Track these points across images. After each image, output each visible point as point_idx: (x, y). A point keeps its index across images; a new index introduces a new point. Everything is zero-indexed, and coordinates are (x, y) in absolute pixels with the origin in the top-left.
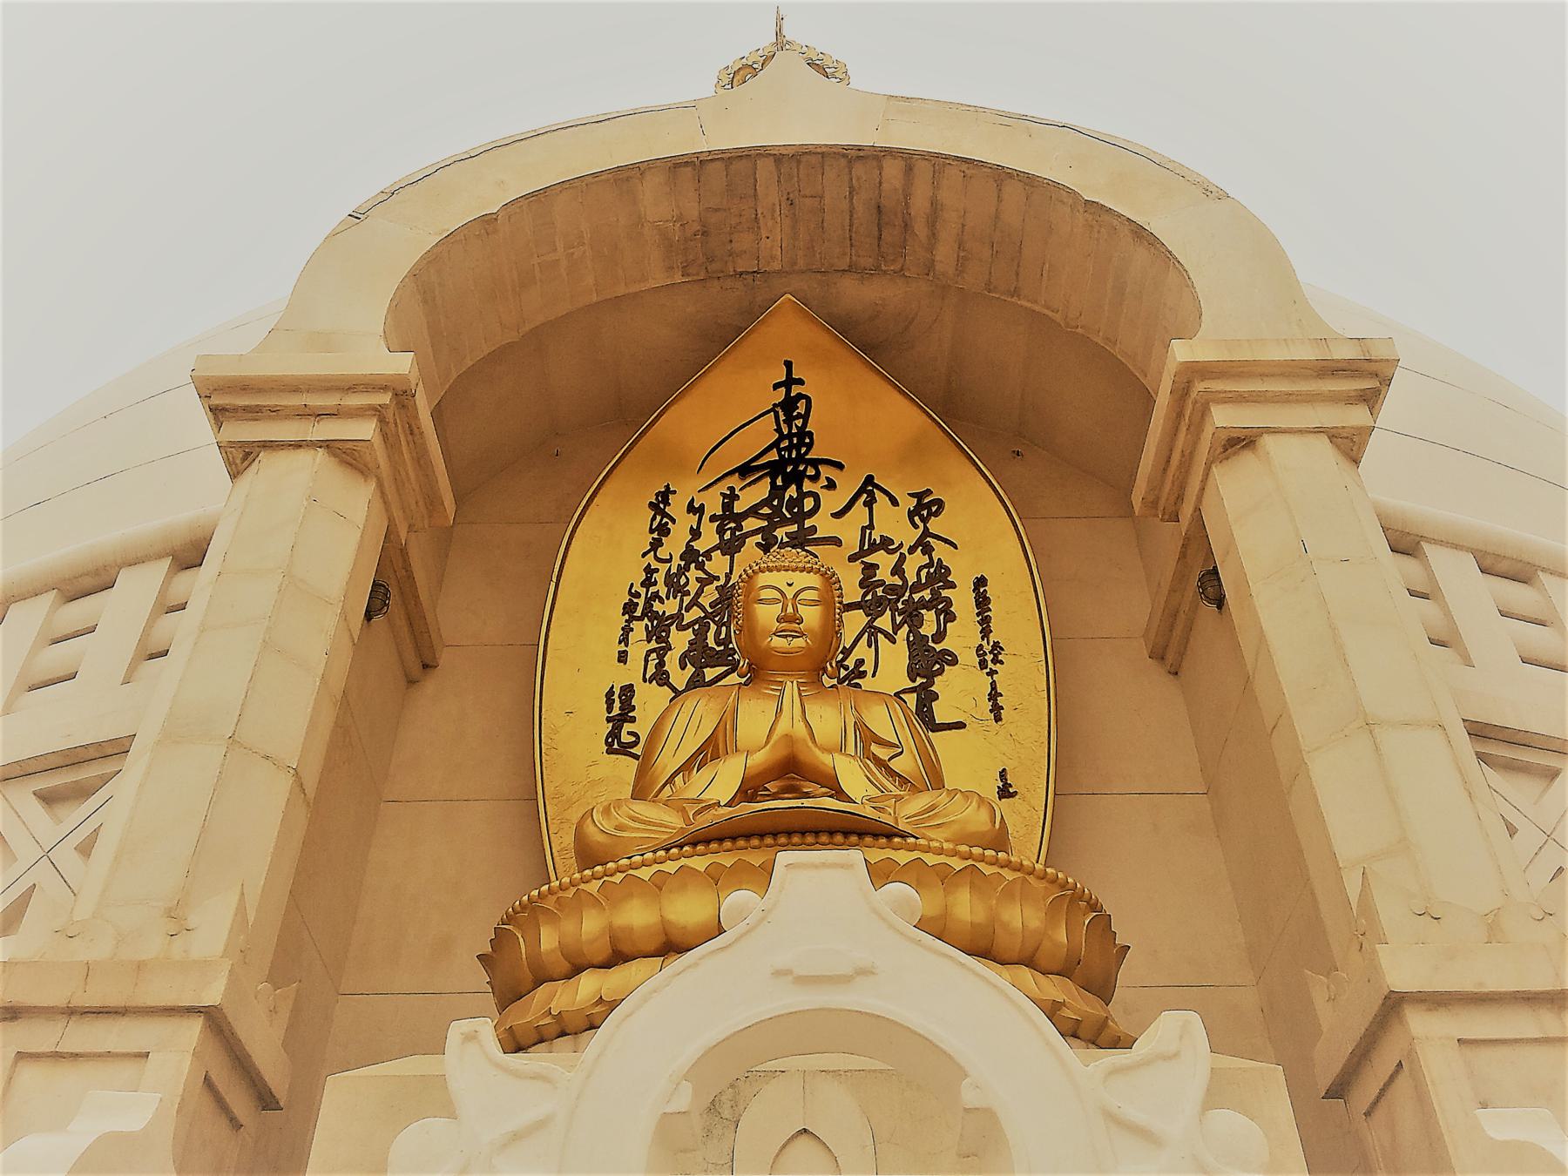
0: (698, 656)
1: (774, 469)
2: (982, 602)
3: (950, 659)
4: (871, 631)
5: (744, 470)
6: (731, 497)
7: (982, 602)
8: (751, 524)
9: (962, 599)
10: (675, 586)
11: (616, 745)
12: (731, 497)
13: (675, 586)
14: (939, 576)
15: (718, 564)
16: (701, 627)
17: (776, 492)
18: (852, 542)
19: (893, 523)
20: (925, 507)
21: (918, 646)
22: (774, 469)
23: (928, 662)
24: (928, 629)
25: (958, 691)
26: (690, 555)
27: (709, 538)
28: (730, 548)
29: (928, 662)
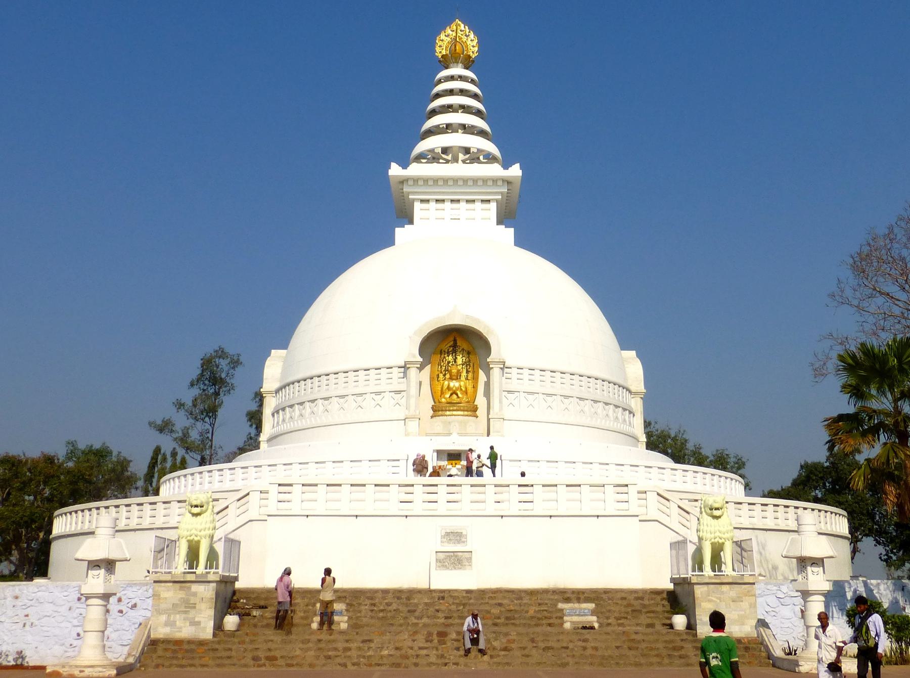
0: (445, 370)
20: (469, 353)
29: (467, 372)
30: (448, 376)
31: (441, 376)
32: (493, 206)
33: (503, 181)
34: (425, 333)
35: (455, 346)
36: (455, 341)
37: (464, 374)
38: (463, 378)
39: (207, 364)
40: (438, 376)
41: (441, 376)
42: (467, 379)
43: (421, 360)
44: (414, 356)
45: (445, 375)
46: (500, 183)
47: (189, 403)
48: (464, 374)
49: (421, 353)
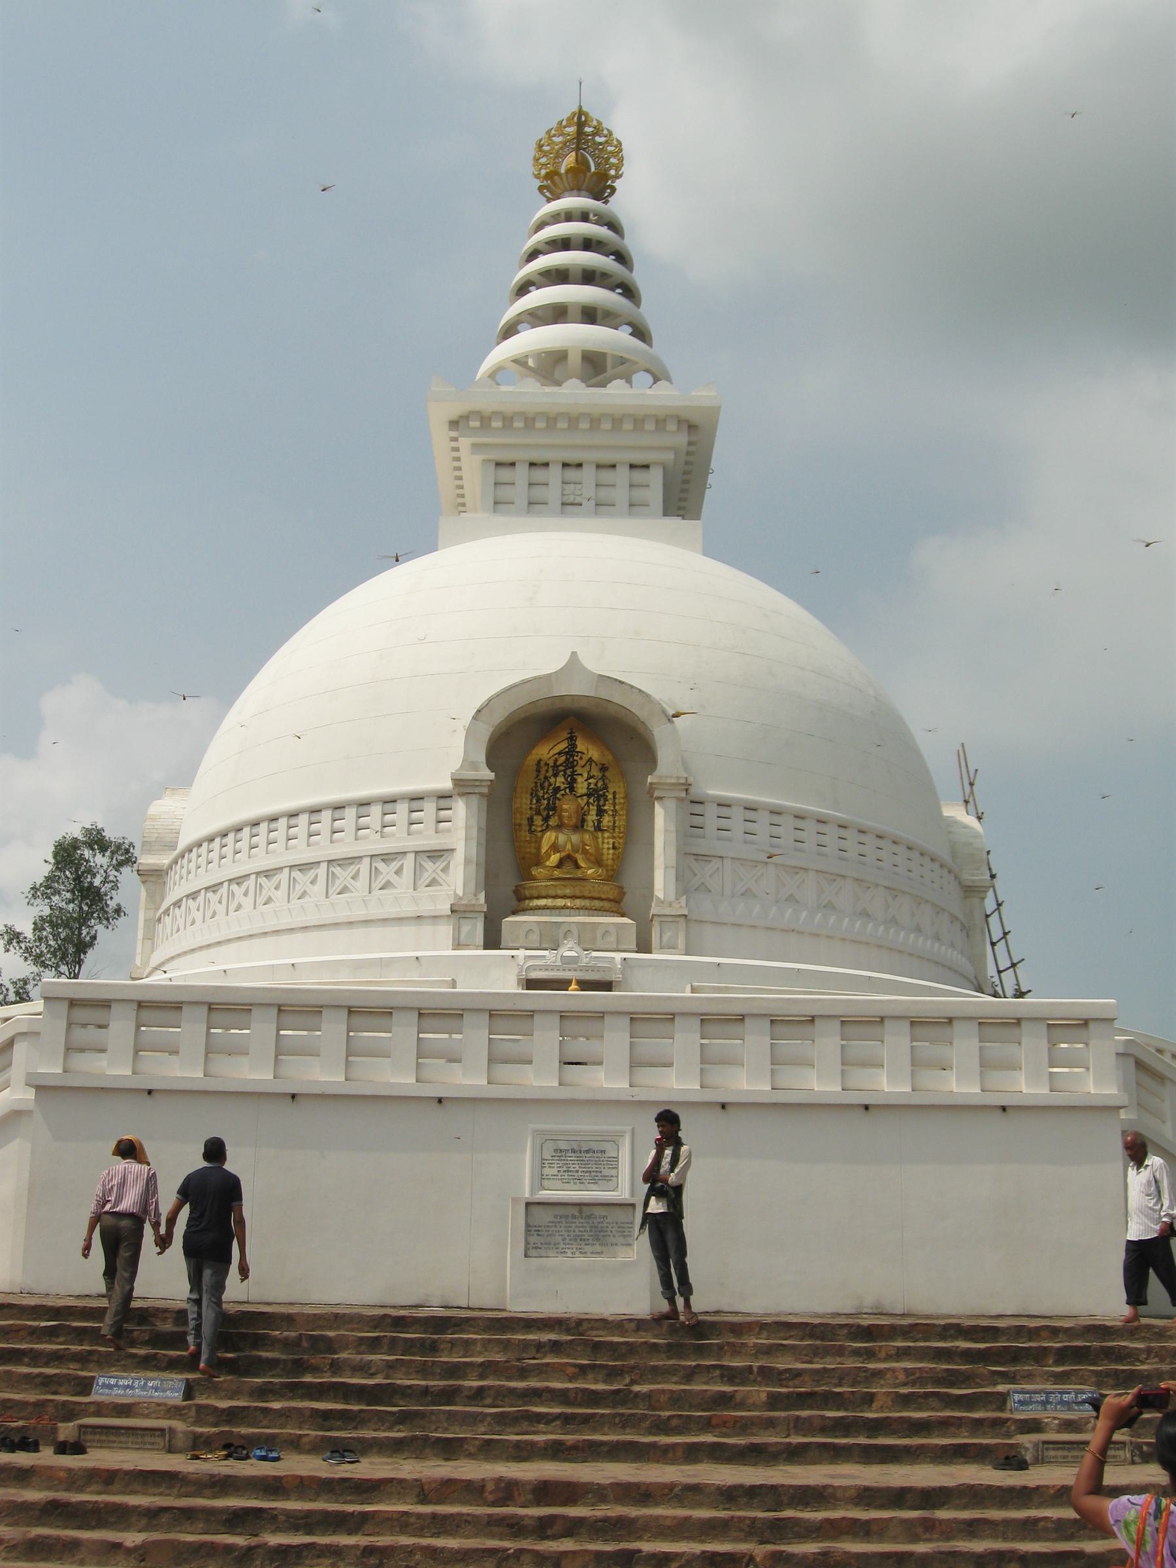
0: (548, 808)
1: (566, 753)
2: (614, 798)
3: (605, 811)
4: (588, 803)
5: (559, 753)
6: (556, 760)
7: (614, 798)
8: (561, 768)
9: (610, 796)
10: (542, 788)
11: (531, 832)
12: (556, 760)
13: (542, 788)
14: (606, 787)
15: (552, 780)
16: (549, 799)
17: (567, 759)
18: (585, 775)
19: (595, 772)
20: (603, 768)
21: (599, 806)
22: (566, 753)
23: (601, 812)
24: (602, 803)
25: (606, 820)
26: (546, 778)
27: (550, 773)
28: (555, 775)
29: (601, 812)
30: (552, 822)
31: (538, 820)
32: (655, 478)
33: (680, 421)
34: (499, 716)
35: (571, 752)
36: (572, 739)
37: (592, 817)
38: (590, 826)
39: (66, 854)
40: (531, 820)
41: (538, 820)
42: (598, 828)
43: (492, 776)
44: (474, 766)
45: (546, 819)
46: (672, 426)
47: (27, 929)
48: (592, 817)
49: (490, 764)
